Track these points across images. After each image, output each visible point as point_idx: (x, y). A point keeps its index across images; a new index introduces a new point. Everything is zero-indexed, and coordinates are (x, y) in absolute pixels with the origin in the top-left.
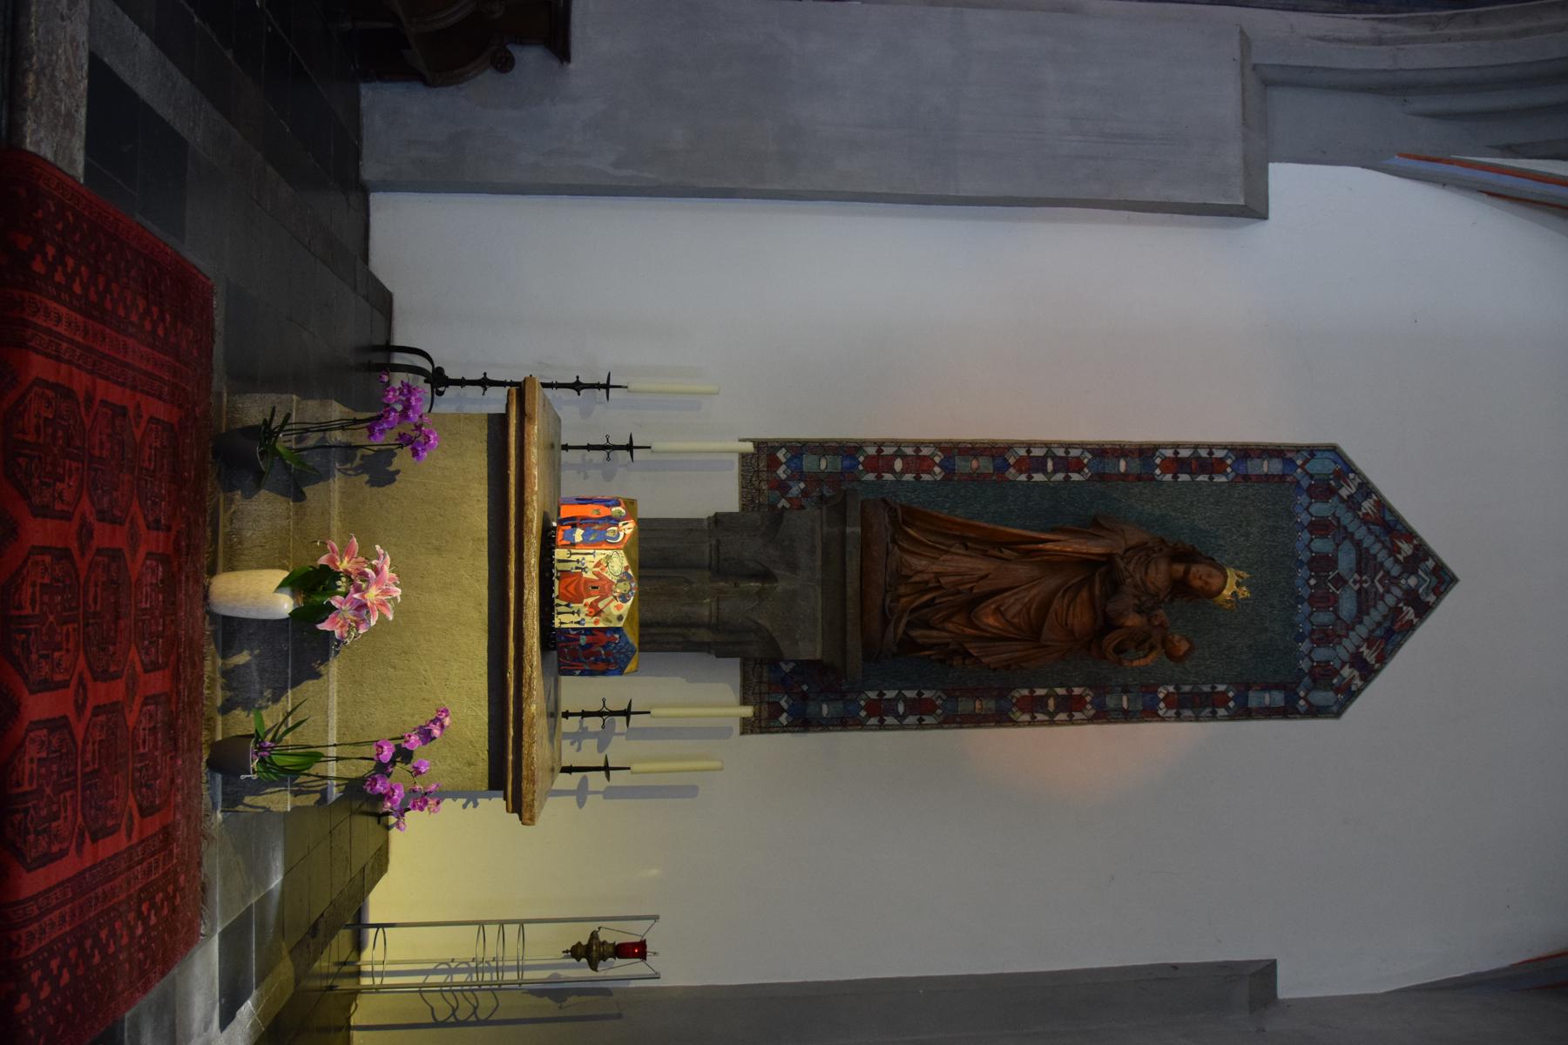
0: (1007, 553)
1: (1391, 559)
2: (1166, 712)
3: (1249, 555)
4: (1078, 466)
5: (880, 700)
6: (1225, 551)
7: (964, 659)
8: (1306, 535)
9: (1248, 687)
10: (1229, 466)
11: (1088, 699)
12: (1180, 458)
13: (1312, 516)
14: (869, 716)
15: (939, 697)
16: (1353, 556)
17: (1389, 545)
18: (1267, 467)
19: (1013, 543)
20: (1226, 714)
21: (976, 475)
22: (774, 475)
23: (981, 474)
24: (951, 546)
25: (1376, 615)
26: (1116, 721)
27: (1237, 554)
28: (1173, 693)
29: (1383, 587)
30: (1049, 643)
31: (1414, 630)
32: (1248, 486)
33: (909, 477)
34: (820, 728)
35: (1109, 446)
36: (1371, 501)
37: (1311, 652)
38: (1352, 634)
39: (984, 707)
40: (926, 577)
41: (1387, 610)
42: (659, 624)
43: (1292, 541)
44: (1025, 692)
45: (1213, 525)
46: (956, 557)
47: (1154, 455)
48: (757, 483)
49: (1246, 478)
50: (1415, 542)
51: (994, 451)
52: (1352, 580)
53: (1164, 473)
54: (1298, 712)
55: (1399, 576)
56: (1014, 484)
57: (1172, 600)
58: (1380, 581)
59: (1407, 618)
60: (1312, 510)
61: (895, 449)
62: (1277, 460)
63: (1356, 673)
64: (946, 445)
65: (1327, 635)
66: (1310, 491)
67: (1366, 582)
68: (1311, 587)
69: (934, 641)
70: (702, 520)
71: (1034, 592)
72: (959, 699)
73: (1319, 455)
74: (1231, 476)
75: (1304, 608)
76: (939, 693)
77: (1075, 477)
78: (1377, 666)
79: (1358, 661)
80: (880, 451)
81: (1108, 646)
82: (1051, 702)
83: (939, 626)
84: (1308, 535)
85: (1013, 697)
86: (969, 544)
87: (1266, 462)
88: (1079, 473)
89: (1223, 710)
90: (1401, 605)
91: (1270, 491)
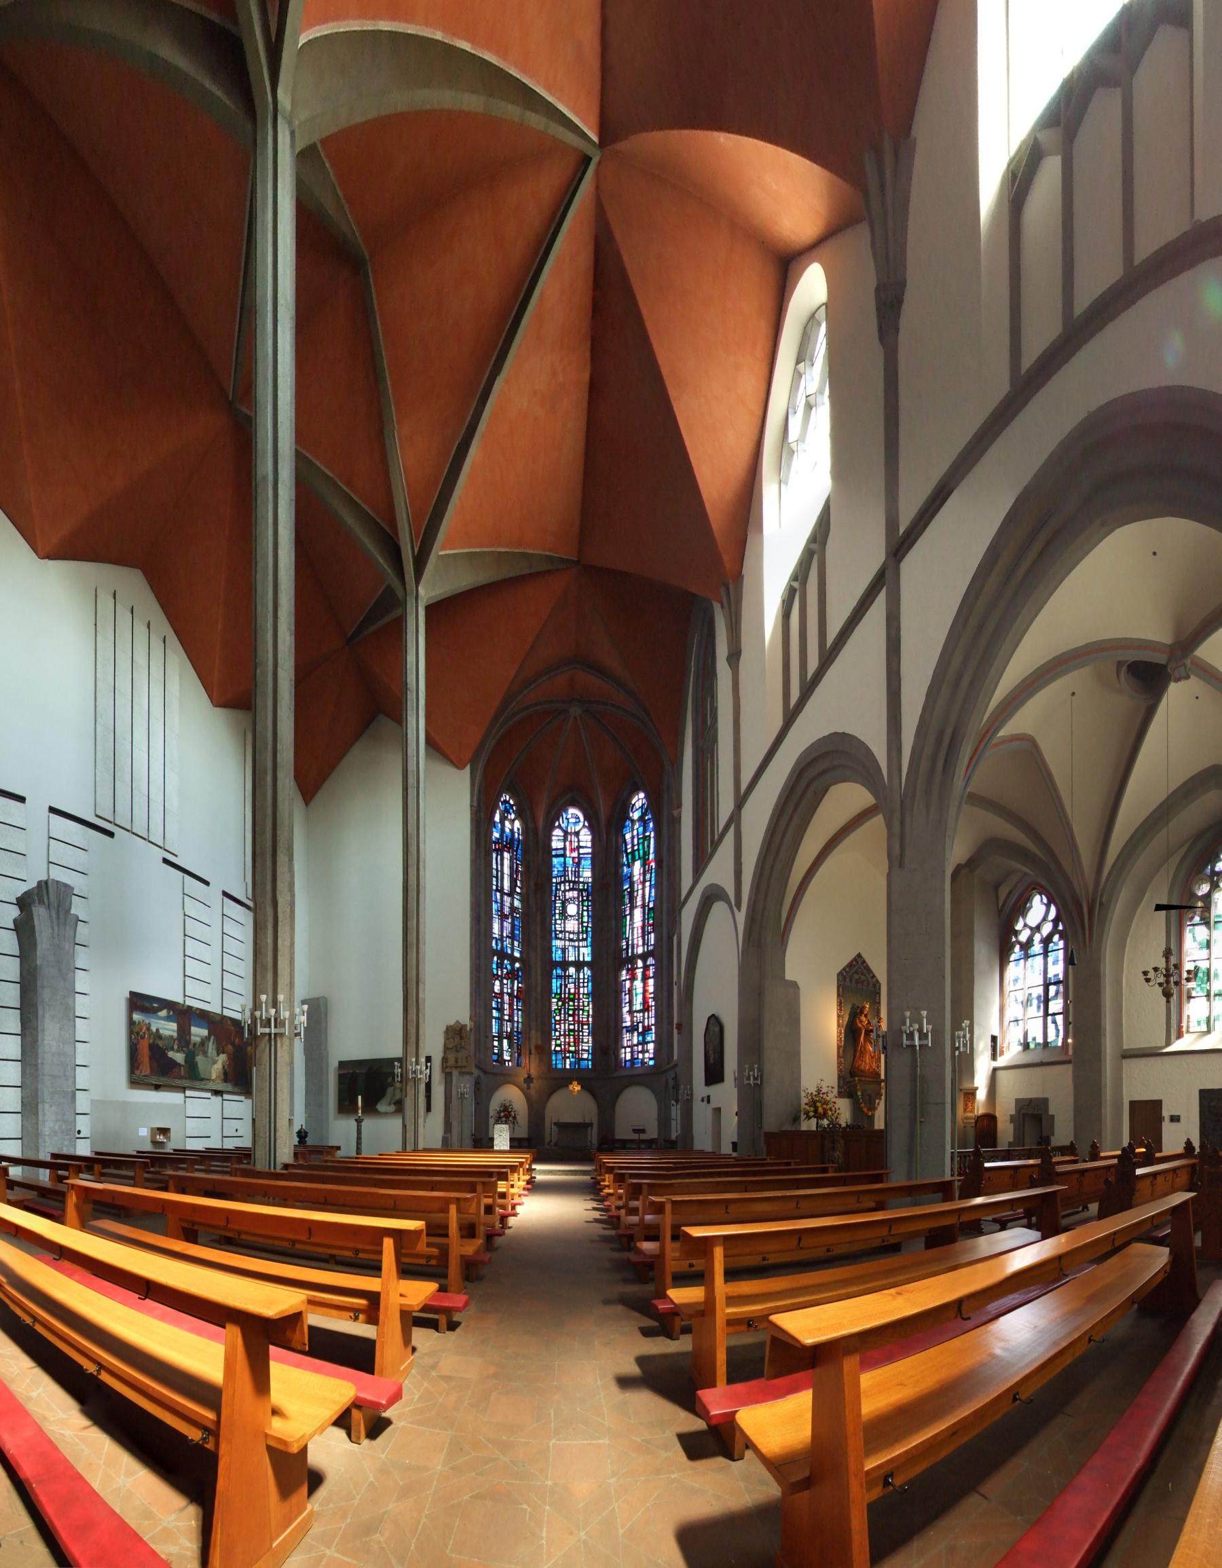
18: (841, 990)
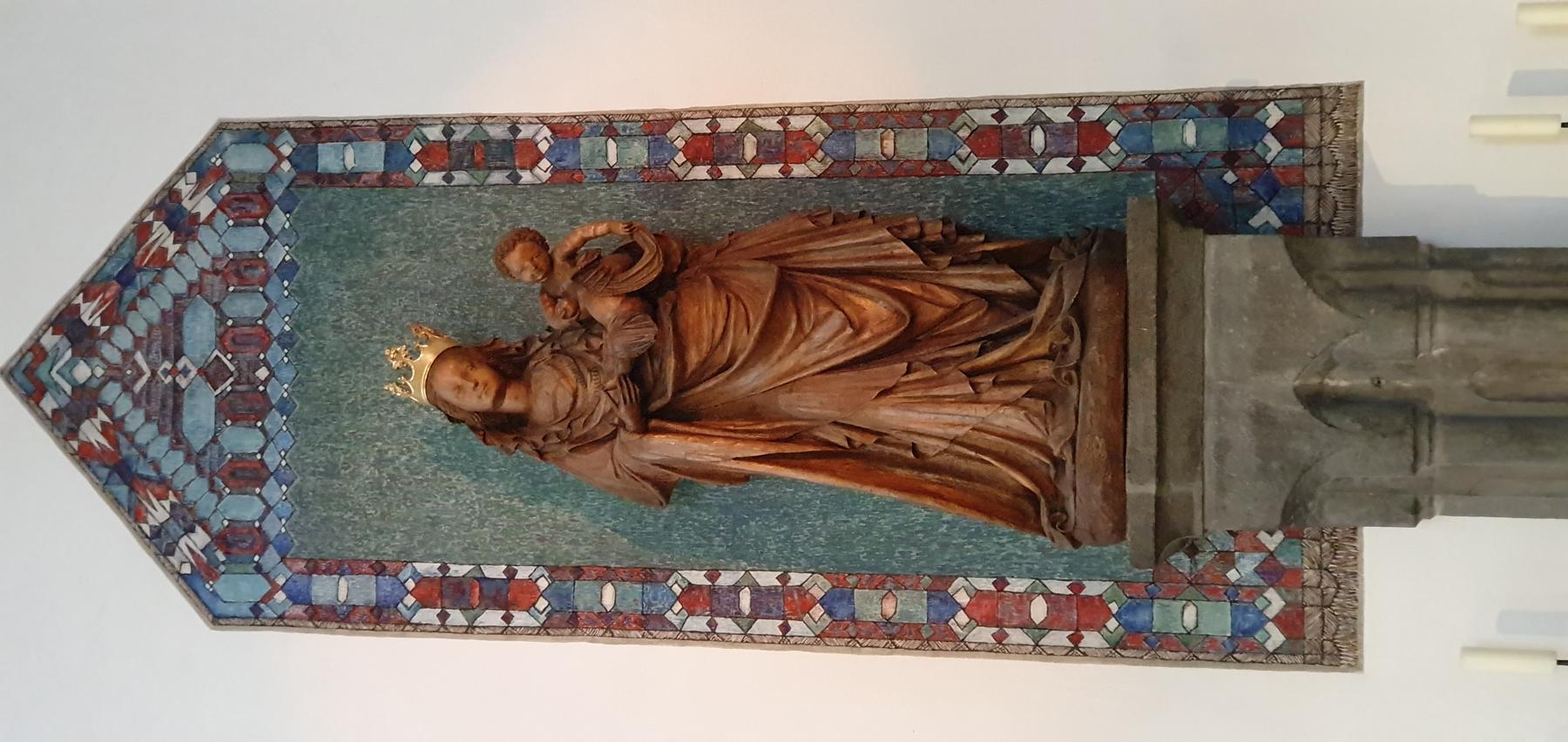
0: (838, 438)
1: (118, 414)
2: (536, 134)
3: (377, 424)
4: (692, 598)
5: (1079, 154)
6: (421, 433)
7: (922, 235)
8: (272, 459)
9: (384, 180)
10: (408, 592)
11: (680, 158)
12: (501, 608)
13: (259, 495)
14: (1100, 124)
16: (188, 421)
17: (122, 440)
19: (828, 456)
20: (425, 130)
21: (888, 585)
22: (1289, 598)
23: (876, 588)
25: (150, 311)
26: (628, 117)
27: (401, 427)
28: (523, 168)
29: (135, 362)
31: (82, 283)
33: (1017, 585)
34: (1200, 98)
35: (633, 633)
36: (152, 521)
37: (269, 244)
38: (194, 277)
40: (998, 394)
41: (130, 321)
42: (1543, 305)
43: (298, 449)
44: (798, 170)
45: (443, 481)
46: (939, 431)
47: (549, 616)
48: (1325, 583)
49: (379, 569)
50: (75, 444)
51: (852, 631)
52: (192, 375)
53: (532, 582)
54: (292, 131)
55: (104, 384)
56: (815, 567)
57: (527, 343)
58: (141, 374)
59: (95, 304)
60: (259, 507)
62: (321, 601)
63: (187, 204)
64: (943, 645)
65: (238, 273)
66: (261, 541)
67: (166, 373)
68: (266, 363)
69: (979, 271)
70: (1446, 512)
71: (789, 363)
72: (924, 157)
73: (245, 610)
74: (406, 573)
75: (279, 325)
76: (963, 168)
77: (698, 578)
78: (150, 218)
79: (184, 226)
80: (1076, 639)
81: (651, 262)
82: (750, 151)
83: (968, 298)
84: (267, 459)
86: (911, 455)
87: (342, 597)
88: (690, 583)
89: (431, 138)
90: (104, 329)
91: (336, 544)
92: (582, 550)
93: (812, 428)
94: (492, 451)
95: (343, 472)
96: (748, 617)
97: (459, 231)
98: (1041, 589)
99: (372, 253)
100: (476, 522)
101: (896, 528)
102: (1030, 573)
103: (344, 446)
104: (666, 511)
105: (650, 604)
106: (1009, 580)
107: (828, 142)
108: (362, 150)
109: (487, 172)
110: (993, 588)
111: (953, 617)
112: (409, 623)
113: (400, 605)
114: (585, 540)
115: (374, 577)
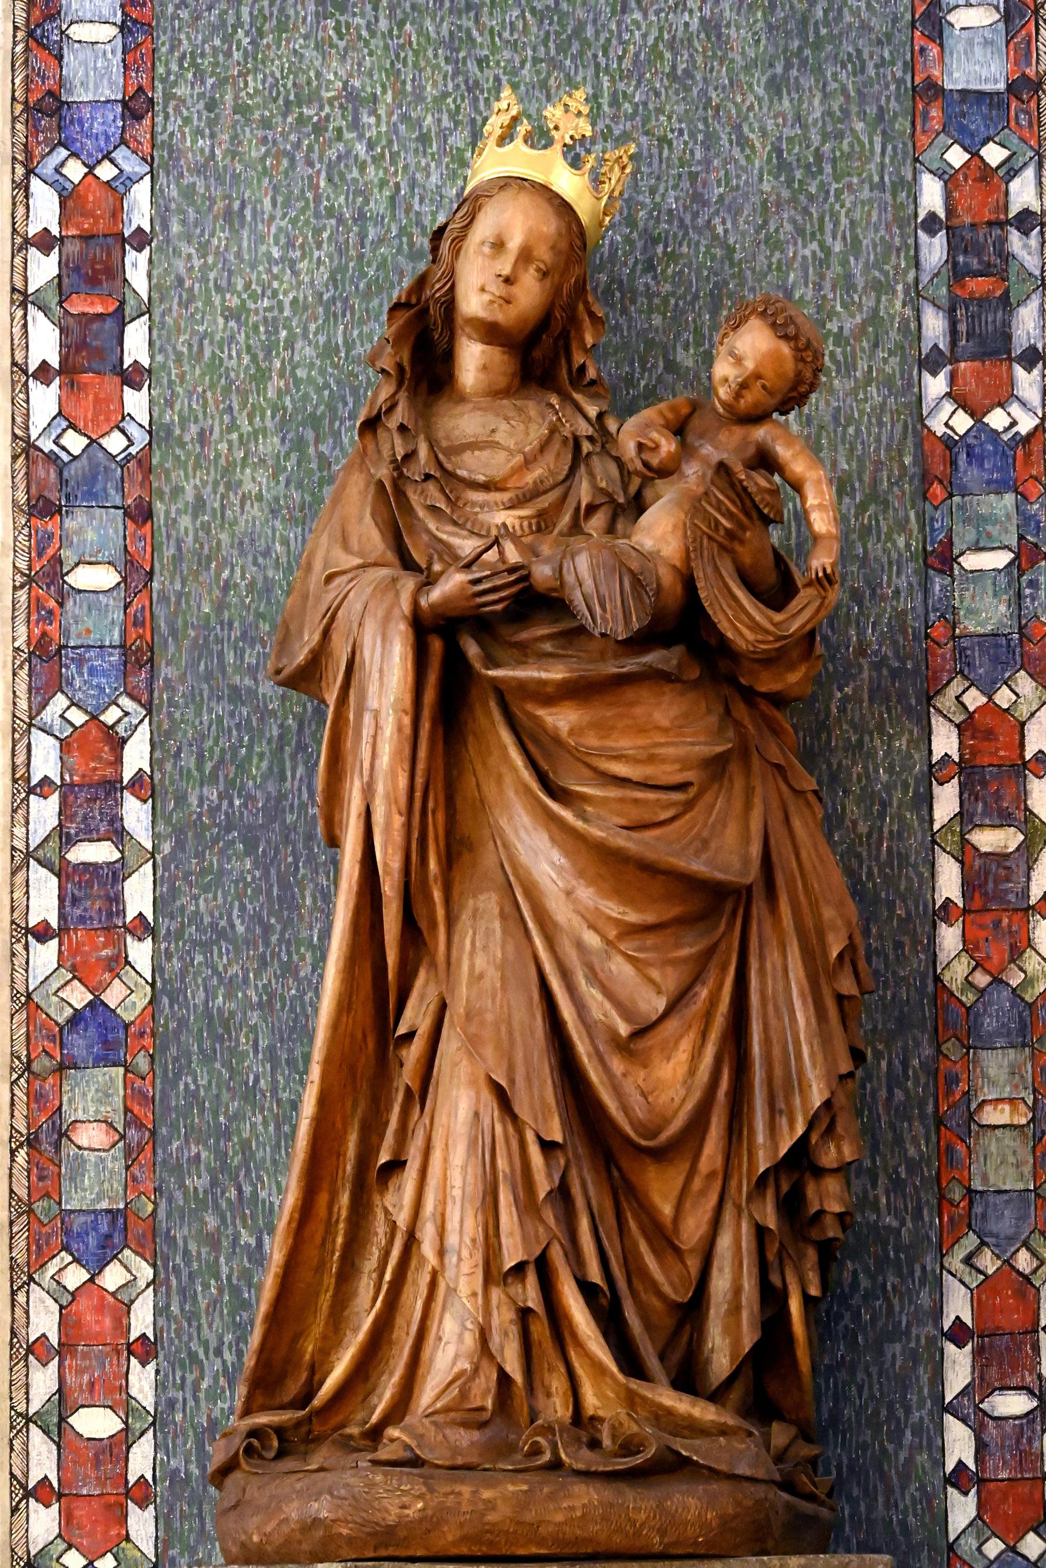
2: (1023, 404)
5: (981, 1482)
6: (413, 184)
7: (819, 1172)
9: (932, 90)
10: (91, 168)
11: (974, 699)
12: (64, 360)
15: (968, 1260)
20: (1030, 173)
21: (132, 1133)
23: (127, 1110)
24: (393, 1226)
27: (424, 139)
28: (953, 378)
30: (755, 850)
32: (168, 96)
35: (22, 630)
39: (1007, 1093)
40: (503, 1318)
45: (318, 232)
46: (429, 1205)
47: (51, 458)
61: (35, 1432)
64: (21, 1243)
69: (749, 1285)
72: (977, 1185)
74: (129, 162)
76: (955, 1261)
80: (42, 1492)
83: (693, 1264)
85: (968, 983)
86: (384, 1158)
87: (77, 32)
88: (124, 741)
89: (1014, 186)
91: (184, 14)
92: (185, 521)
93: (433, 965)
94: (379, 328)
95: (331, 23)
96: (62, 858)
97: (827, 251)
98: (137, 1426)
99: (779, 69)
100: (234, 302)
101: (245, 1146)
102: (166, 1406)
103: (383, 25)
104: (267, 688)
105: (80, 661)
106: (151, 1367)
107: (1006, 993)
108: (987, 43)
109: (944, 302)
110: (134, 1335)
111: (76, 1260)
112: (30, 172)
113: (63, 153)
114: (206, 528)
115: (120, 97)
